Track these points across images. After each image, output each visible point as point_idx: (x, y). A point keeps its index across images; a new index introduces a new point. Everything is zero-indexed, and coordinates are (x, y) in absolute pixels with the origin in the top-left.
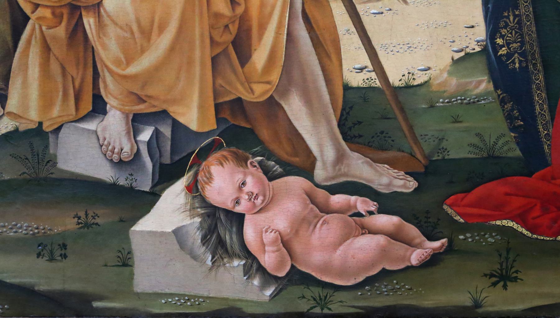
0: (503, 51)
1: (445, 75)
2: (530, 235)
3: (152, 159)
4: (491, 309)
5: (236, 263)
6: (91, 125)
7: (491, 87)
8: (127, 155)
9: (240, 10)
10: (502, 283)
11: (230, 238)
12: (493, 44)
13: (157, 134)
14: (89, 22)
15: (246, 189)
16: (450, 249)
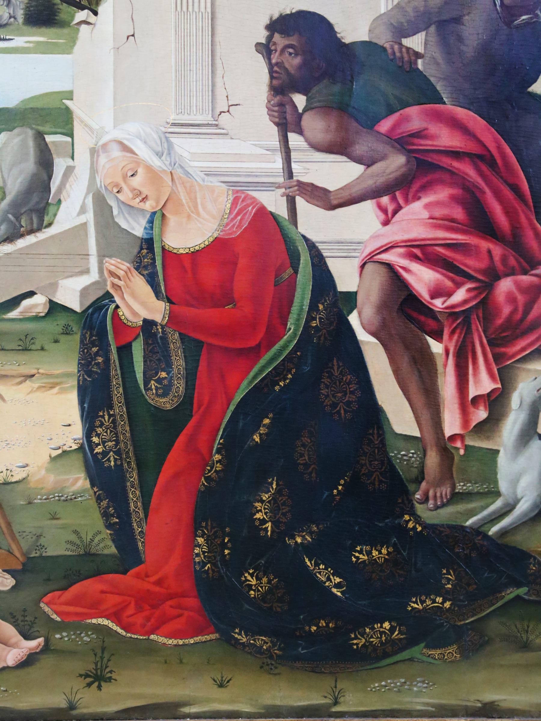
0: (99, 449)
1: (43, 472)
4: (85, 711)
7: (88, 484)
10: (96, 684)
12: (90, 442)
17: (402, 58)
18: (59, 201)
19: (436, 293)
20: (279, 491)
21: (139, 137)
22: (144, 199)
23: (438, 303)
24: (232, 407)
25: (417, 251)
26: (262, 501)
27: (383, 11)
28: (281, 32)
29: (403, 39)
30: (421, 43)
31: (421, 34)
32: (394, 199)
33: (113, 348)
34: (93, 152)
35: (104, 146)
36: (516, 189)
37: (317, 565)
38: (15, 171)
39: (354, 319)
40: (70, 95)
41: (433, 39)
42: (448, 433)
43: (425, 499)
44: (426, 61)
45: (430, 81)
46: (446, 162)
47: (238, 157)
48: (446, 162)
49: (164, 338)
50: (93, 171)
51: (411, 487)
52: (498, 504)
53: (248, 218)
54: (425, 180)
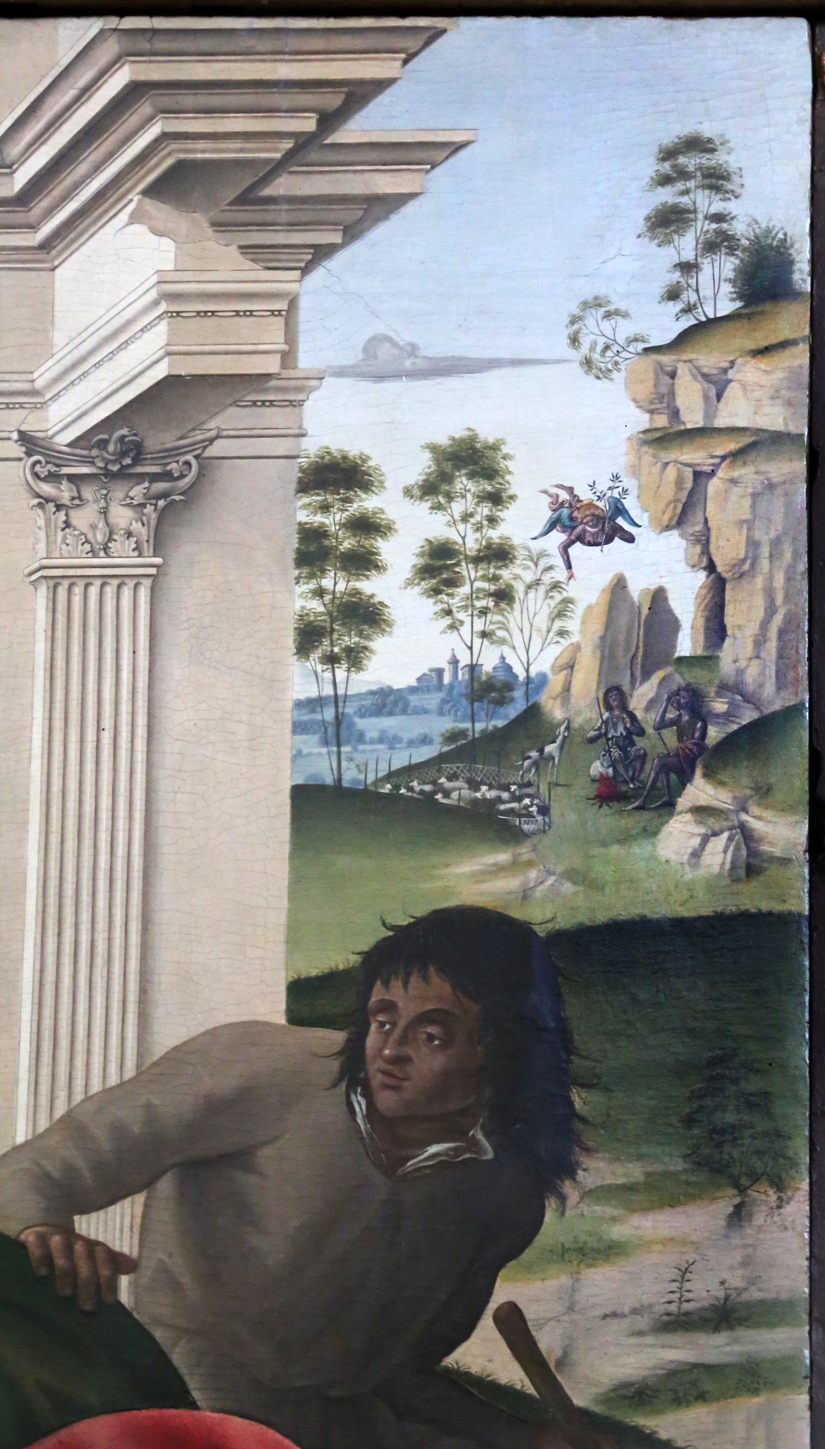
17: (72, 1273)
27: (20, 1139)
29: (76, 1218)
30: (132, 1227)
31: (133, 1203)
41: (165, 1215)
44: (145, 1281)
45: (151, 1339)
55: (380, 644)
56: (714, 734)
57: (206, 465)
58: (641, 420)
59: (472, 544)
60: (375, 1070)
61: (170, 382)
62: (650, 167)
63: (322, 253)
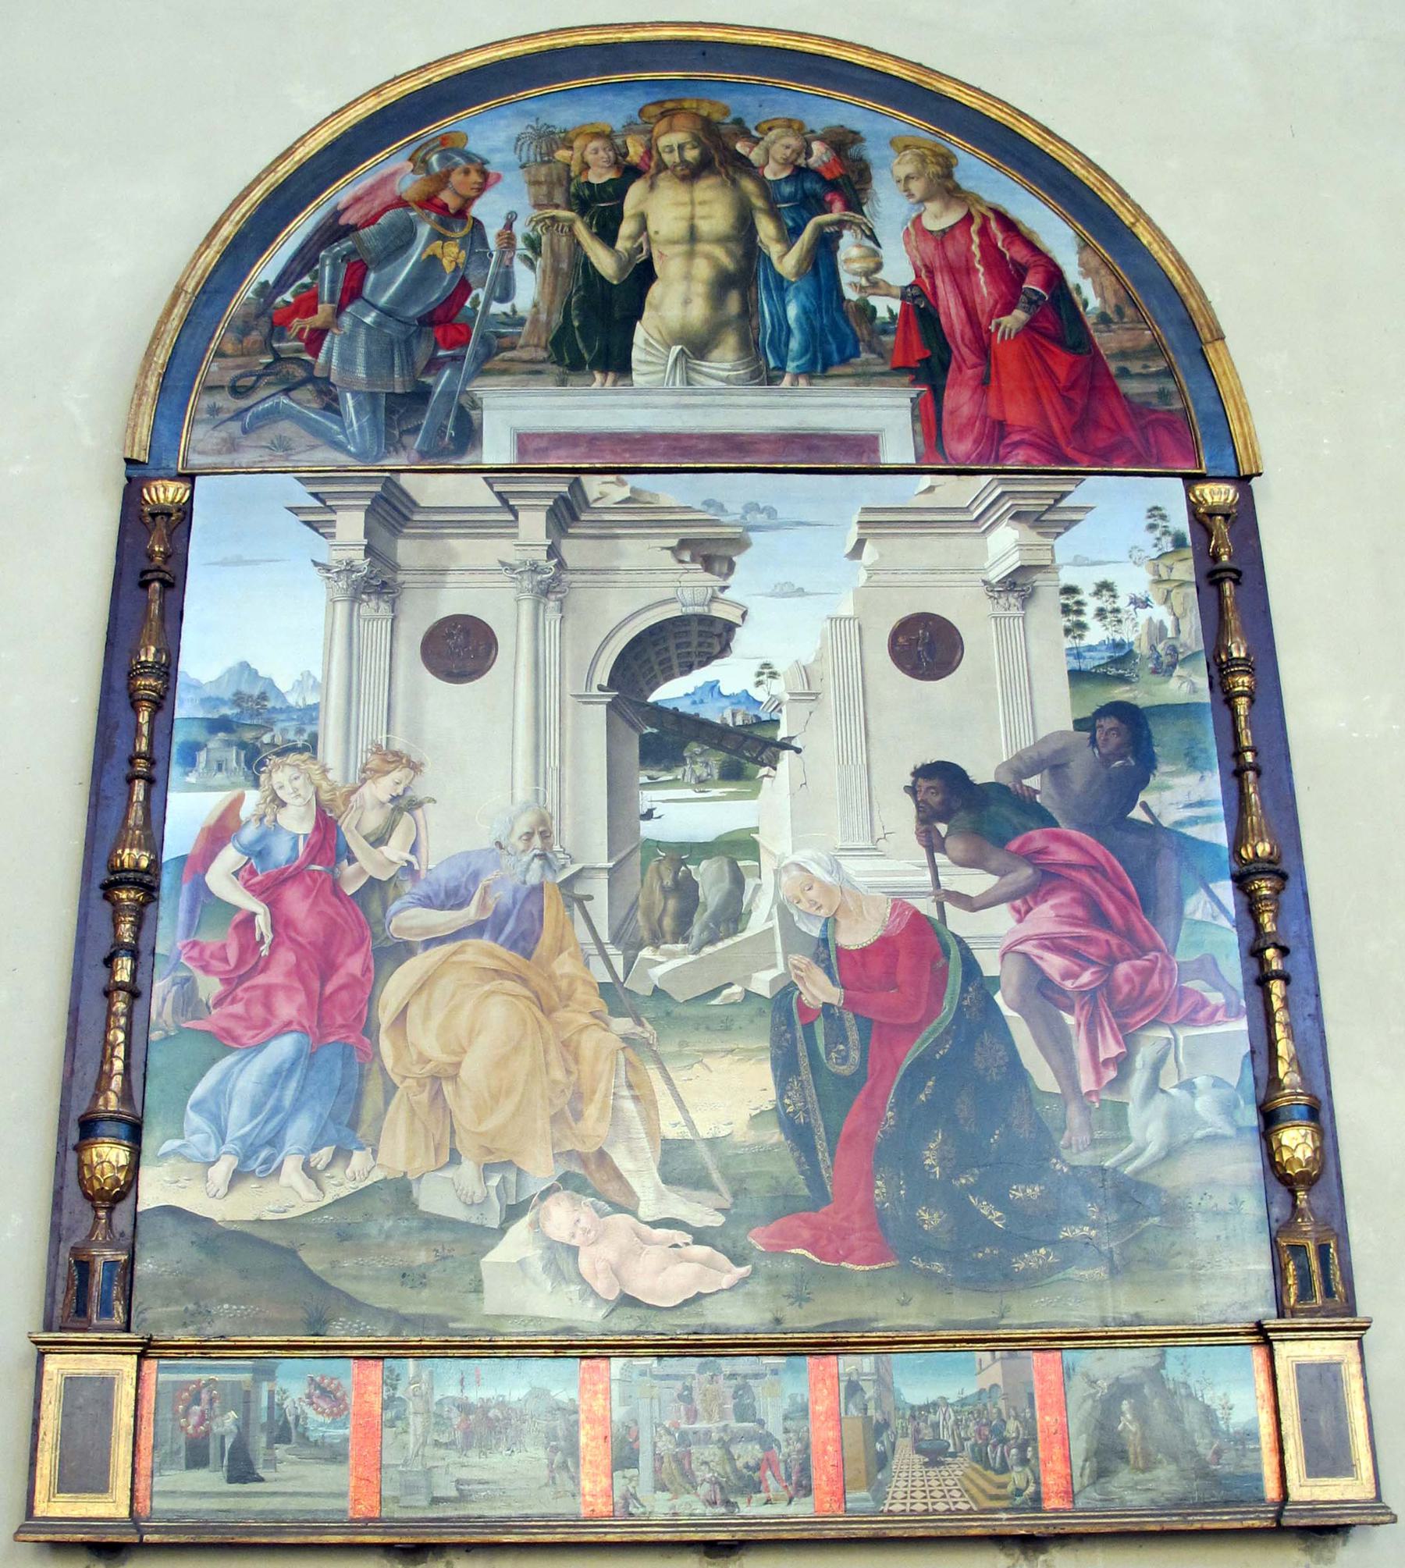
0: (790, 1109)
2: (817, 1260)
3: (499, 1199)
5: (573, 1288)
6: (448, 1173)
7: (783, 1138)
8: (477, 1200)
9: (573, 1078)
11: (566, 1265)
13: (504, 1179)
14: (448, 1089)
15: (580, 1225)
16: (755, 1271)
18: (750, 912)
19: (1068, 975)
20: (944, 1142)
21: (813, 860)
22: (819, 908)
23: (1069, 984)
24: (901, 1073)
25: (1047, 943)
26: (930, 1149)
28: (924, 777)
32: (1025, 902)
33: (799, 1027)
34: (776, 872)
35: (786, 867)
36: (1124, 892)
37: (980, 1202)
38: (714, 890)
39: (998, 998)
40: (756, 830)
41: (1047, 780)
42: (1084, 1090)
43: (1070, 1146)
46: (1066, 872)
47: (894, 873)
48: (1066, 872)
49: (841, 1018)
50: (777, 886)
51: (1056, 1136)
52: (1132, 1146)
53: (905, 922)
54: (1048, 887)
55: (1086, 633)
56: (1181, 657)
57: (1034, 589)
58: (1151, 577)
59: (1109, 608)
60: (1100, 742)
61: (1022, 567)
62: (1145, 514)
63: (1059, 534)
